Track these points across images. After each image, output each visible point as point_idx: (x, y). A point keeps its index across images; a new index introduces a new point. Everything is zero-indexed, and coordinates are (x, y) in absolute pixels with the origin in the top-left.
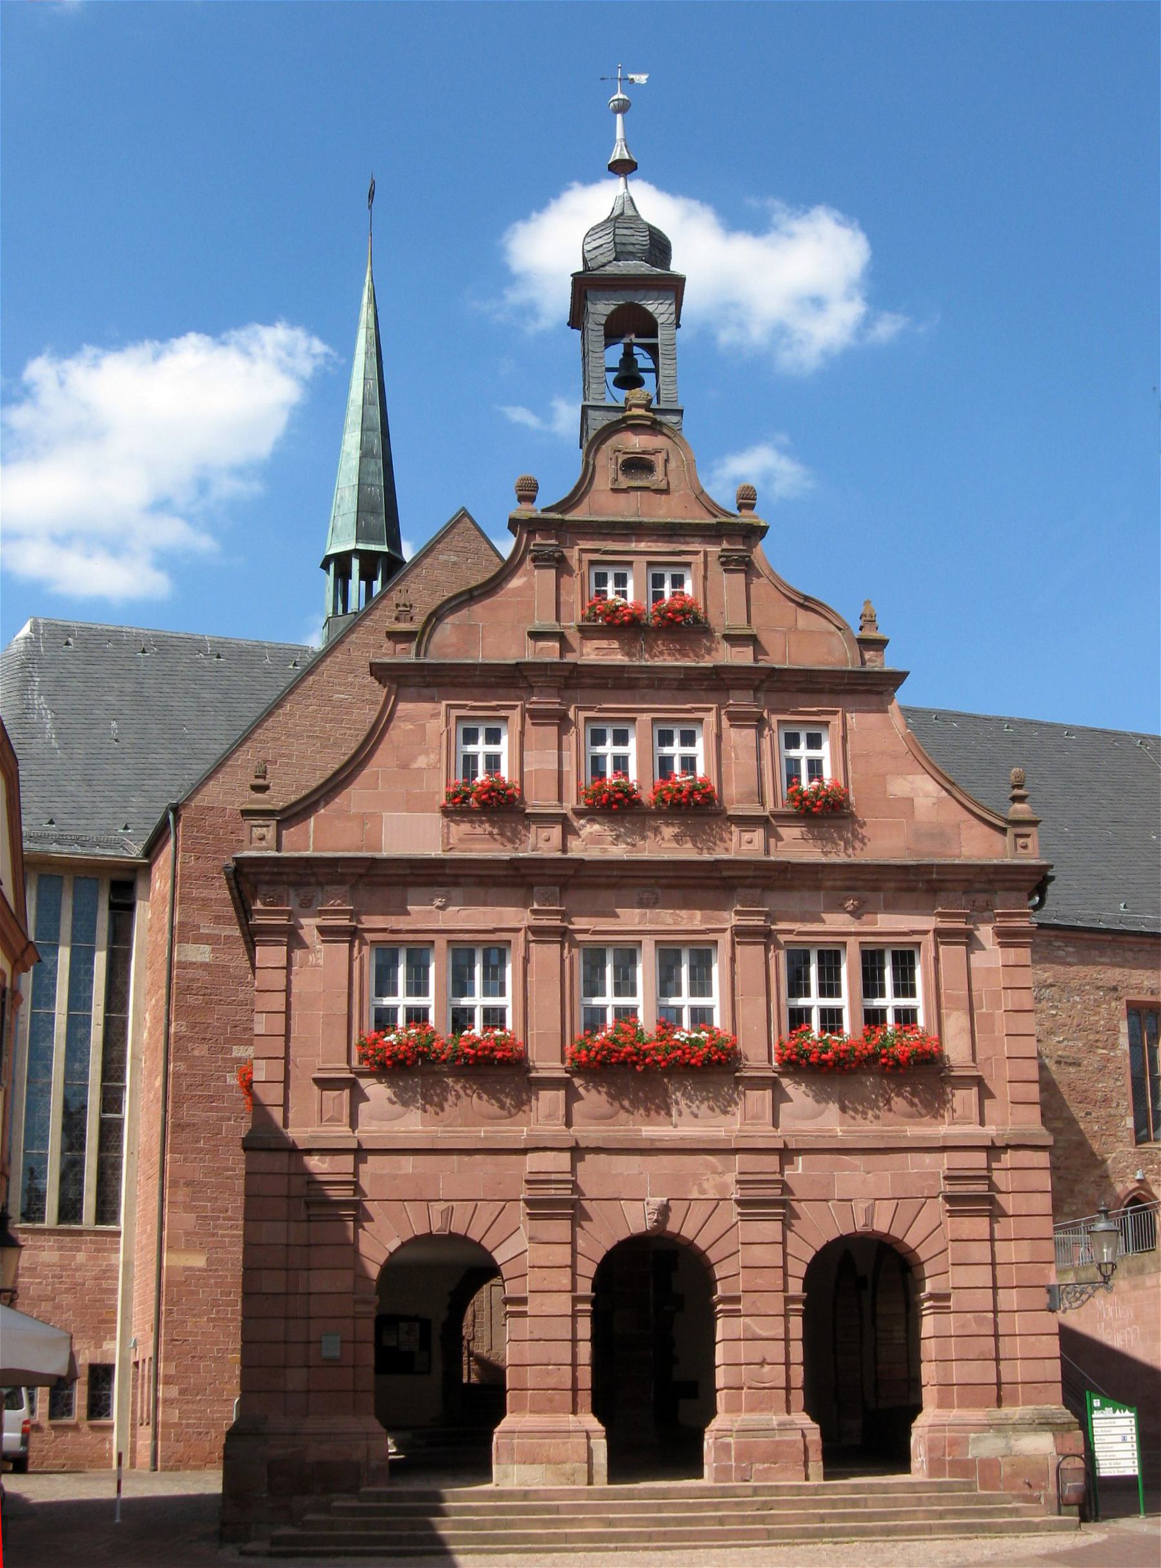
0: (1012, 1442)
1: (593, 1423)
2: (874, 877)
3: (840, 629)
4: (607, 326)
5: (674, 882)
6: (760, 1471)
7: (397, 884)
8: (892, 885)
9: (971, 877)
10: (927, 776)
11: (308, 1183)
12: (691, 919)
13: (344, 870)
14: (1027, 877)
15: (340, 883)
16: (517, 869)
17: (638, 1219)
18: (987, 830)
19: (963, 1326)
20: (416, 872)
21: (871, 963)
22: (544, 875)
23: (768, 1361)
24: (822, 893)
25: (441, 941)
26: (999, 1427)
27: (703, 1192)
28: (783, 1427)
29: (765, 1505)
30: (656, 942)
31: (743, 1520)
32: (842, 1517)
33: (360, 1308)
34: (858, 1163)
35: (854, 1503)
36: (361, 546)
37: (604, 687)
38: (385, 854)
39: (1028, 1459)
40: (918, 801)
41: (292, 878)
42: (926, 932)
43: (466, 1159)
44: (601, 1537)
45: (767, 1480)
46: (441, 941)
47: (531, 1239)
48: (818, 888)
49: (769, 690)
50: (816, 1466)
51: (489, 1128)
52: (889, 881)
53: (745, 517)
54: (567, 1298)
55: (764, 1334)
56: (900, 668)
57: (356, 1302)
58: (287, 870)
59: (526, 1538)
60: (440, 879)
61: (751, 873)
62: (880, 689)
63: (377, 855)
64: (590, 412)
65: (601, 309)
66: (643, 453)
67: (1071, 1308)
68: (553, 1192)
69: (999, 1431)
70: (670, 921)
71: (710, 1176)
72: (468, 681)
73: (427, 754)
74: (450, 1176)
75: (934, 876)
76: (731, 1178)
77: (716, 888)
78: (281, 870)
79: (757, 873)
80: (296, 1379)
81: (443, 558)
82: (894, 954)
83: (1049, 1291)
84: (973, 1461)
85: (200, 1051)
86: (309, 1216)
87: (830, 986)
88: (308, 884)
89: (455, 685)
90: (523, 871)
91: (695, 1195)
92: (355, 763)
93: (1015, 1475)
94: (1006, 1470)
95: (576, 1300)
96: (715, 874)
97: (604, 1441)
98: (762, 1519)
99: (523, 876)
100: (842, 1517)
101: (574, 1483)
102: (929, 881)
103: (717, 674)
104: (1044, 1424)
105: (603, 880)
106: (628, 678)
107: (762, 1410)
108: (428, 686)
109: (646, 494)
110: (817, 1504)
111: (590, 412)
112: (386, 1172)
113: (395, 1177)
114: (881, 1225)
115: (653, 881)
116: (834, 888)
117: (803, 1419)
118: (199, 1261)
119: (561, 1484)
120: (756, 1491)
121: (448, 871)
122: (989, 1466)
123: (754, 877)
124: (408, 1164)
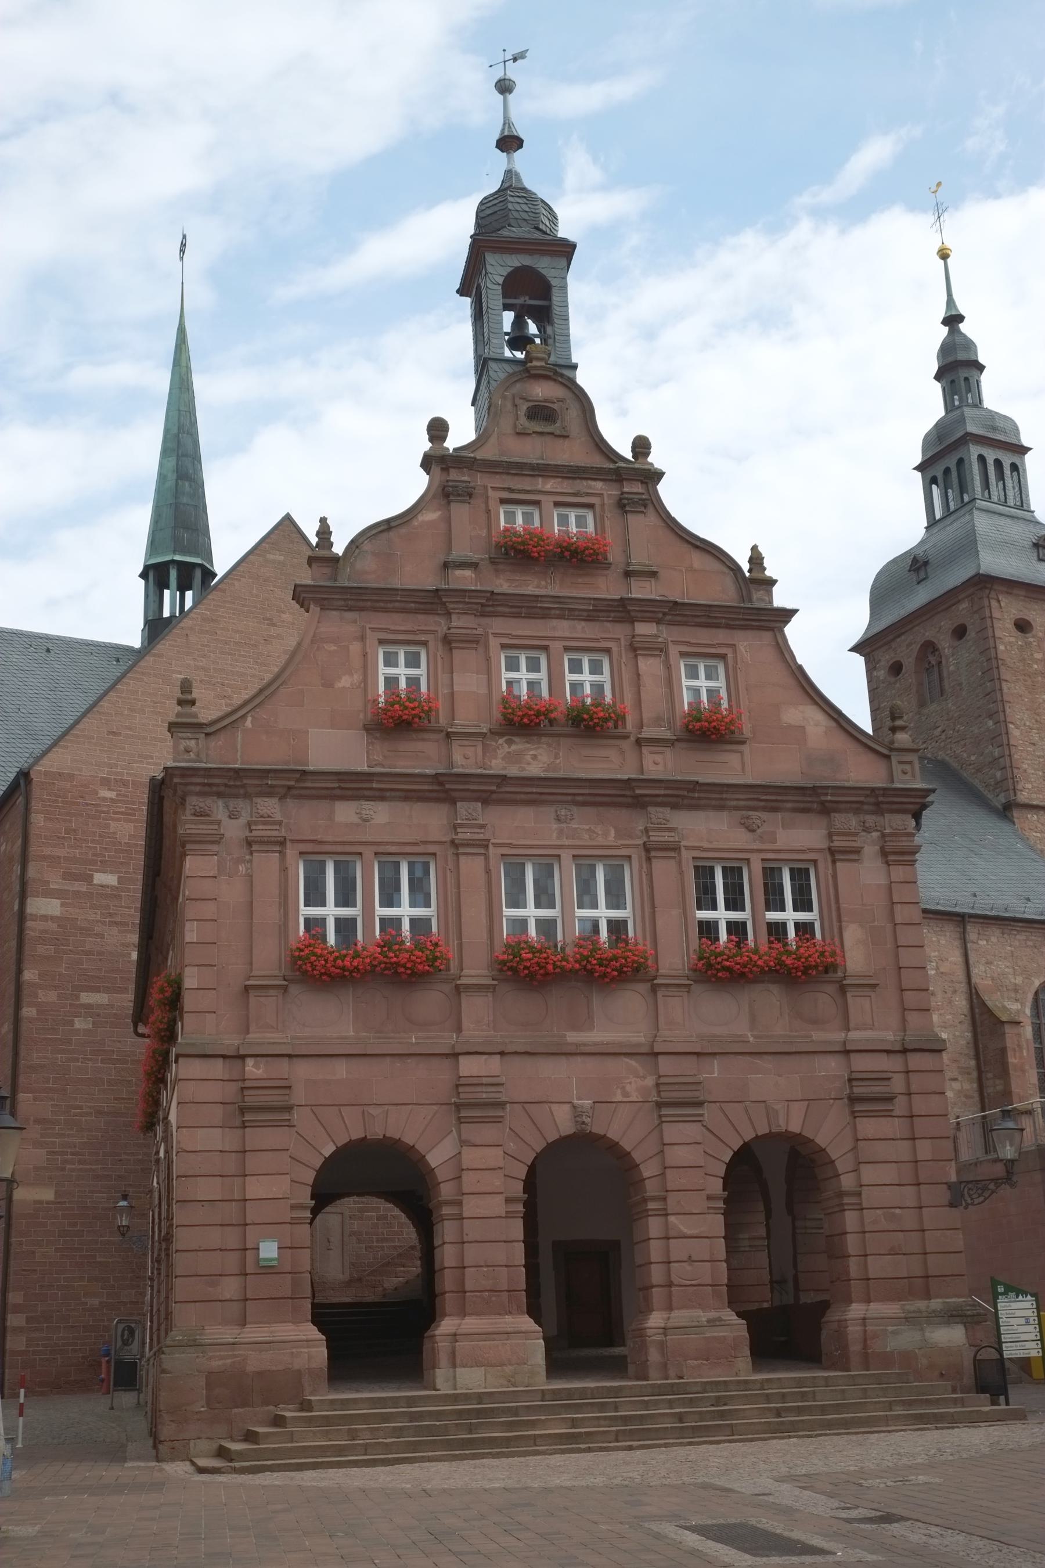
0: (927, 1334)
1: (527, 1323)
3: (732, 570)
4: (504, 286)
8: (789, 805)
9: (862, 799)
10: (815, 707)
11: (242, 1089)
13: (274, 783)
14: (912, 800)
15: (270, 795)
16: (441, 784)
17: (563, 1123)
18: (871, 756)
20: (343, 785)
21: (771, 874)
22: (468, 790)
23: (694, 1258)
24: (725, 813)
26: (911, 1320)
27: (626, 1094)
28: (712, 1323)
29: (718, 1401)
32: (800, 1411)
35: (803, 1396)
36: (177, 558)
37: (517, 616)
38: (311, 768)
40: (811, 730)
41: (222, 789)
42: (821, 850)
44: (507, 1442)
46: (368, 852)
47: (463, 1143)
48: (721, 808)
49: (671, 623)
50: (743, 1362)
51: (419, 1034)
54: (500, 1199)
56: (795, 607)
57: (293, 1207)
58: (217, 781)
60: (367, 793)
61: (662, 792)
62: (773, 624)
66: (546, 401)
67: (972, 1204)
68: (484, 1096)
70: (587, 836)
72: (390, 605)
73: (351, 674)
75: (829, 798)
76: (650, 1081)
77: (627, 806)
78: (211, 781)
81: (270, 557)
82: (792, 871)
85: (52, 996)
87: (735, 900)
88: (236, 796)
89: (375, 610)
90: (447, 786)
91: (619, 1098)
92: (266, 693)
95: (508, 1200)
96: (628, 793)
97: (542, 1341)
99: (447, 791)
100: (800, 1411)
102: (823, 803)
103: (624, 606)
104: (952, 1316)
108: (350, 609)
109: (548, 438)
115: (569, 798)
116: (737, 808)
118: (47, 1194)
119: (502, 1386)
121: (374, 785)
122: (907, 1358)
124: (341, 1070)
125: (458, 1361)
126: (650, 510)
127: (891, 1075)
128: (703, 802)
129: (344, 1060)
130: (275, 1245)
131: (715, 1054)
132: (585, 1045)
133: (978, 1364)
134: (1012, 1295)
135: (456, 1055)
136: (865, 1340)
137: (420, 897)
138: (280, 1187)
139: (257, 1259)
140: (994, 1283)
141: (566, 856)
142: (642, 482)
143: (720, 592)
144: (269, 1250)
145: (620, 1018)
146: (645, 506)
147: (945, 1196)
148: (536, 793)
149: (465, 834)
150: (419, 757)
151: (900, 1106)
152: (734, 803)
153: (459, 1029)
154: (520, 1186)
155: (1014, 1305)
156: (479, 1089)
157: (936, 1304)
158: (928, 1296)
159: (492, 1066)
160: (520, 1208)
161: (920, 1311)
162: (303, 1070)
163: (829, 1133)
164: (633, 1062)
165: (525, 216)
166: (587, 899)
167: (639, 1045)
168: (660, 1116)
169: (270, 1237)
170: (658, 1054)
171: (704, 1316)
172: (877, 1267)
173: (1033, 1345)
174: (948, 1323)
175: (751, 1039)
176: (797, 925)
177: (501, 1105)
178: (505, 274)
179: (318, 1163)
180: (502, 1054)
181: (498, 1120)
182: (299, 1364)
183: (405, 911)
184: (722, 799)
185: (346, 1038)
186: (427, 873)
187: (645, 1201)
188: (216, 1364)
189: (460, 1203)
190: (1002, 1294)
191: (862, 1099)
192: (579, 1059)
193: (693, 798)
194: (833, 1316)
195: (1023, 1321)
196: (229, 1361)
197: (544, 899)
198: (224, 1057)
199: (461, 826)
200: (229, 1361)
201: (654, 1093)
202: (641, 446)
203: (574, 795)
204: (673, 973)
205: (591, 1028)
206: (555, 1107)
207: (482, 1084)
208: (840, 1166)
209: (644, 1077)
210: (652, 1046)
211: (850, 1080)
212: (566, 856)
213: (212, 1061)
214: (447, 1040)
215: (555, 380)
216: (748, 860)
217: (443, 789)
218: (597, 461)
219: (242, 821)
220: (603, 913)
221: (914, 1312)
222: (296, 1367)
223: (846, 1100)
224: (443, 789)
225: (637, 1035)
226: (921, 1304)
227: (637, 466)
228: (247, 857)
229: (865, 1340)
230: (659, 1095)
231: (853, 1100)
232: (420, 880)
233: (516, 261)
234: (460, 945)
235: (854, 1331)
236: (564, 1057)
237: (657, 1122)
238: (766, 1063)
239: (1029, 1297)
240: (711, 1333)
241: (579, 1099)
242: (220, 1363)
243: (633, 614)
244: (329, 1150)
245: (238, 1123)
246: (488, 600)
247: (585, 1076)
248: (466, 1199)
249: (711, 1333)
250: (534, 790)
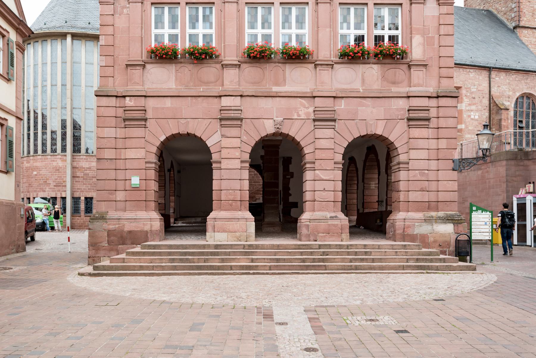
1: (249, 215)
6: (322, 237)
17: (269, 128)
19: (414, 176)
26: (428, 220)
27: (299, 115)
31: (314, 260)
33: (148, 165)
34: (370, 104)
39: (443, 235)
45: (325, 241)
47: (223, 136)
50: (346, 235)
55: (325, 178)
57: (146, 163)
68: (232, 115)
71: (302, 108)
74: (187, 108)
76: (311, 110)
80: (120, 196)
83: (453, 161)
84: (417, 235)
86: (125, 125)
91: (296, 117)
93: (435, 241)
94: (431, 239)
95: (242, 162)
97: (254, 223)
98: (323, 260)
101: (240, 241)
107: (323, 211)
110: (348, 254)
112: (159, 106)
113: (163, 108)
114: (379, 132)
117: (342, 216)
119: (235, 241)
120: (320, 246)
124: (168, 102)
125: (216, 230)
127: (429, 108)
129: (169, 99)
130: (138, 178)
131: (343, 97)
132: (280, 92)
133: (457, 241)
134: (480, 211)
135: (220, 96)
136: (404, 228)
137: (208, 24)
138: (141, 153)
139: (131, 184)
140: (471, 206)
141: (277, 4)
144: (135, 181)
145: (298, 79)
147: (451, 165)
151: (433, 123)
153: (223, 85)
154: (248, 156)
155: (480, 216)
156: (230, 112)
157: (441, 214)
158: (437, 210)
159: (235, 102)
161: (432, 217)
162: (151, 103)
163: (397, 134)
164: (303, 101)
166: (287, 25)
167: (306, 93)
168: (314, 126)
169: (136, 175)
170: (315, 97)
171: (329, 215)
172: (413, 196)
173: (488, 234)
174: (445, 223)
175: (361, 91)
176: (390, 37)
177: (241, 120)
179: (158, 144)
180: (241, 96)
181: (240, 126)
182: (147, 228)
183: (201, 30)
186: (211, 12)
187: (305, 164)
188: (111, 227)
189: (220, 162)
190: (474, 211)
191: (416, 119)
192: (278, 99)
194: (392, 217)
195: (484, 223)
196: (117, 226)
197: (266, 25)
198: (117, 97)
200: (117, 226)
201: (312, 115)
204: (326, 59)
205: (285, 85)
206: (265, 121)
208: (400, 150)
209: (308, 108)
210: (312, 93)
211: (409, 110)
212: (277, 4)
213: (111, 98)
214: (216, 90)
220: (294, 31)
221: (429, 217)
222: (145, 229)
223: (406, 120)
225: (306, 88)
226: (434, 214)
228: (128, 6)
229: (404, 228)
230: (314, 116)
231: (409, 120)
232: (208, 16)
234: (224, 46)
235: (399, 224)
236: (270, 98)
237: (313, 128)
238: (369, 102)
239: (488, 213)
240: (330, 222)
241: (277, 117)
242: (113, 226)
244: (163, 138)
245: (123, 126)
247: (281, 106)
248: (222, 161)
249: (330, 222)
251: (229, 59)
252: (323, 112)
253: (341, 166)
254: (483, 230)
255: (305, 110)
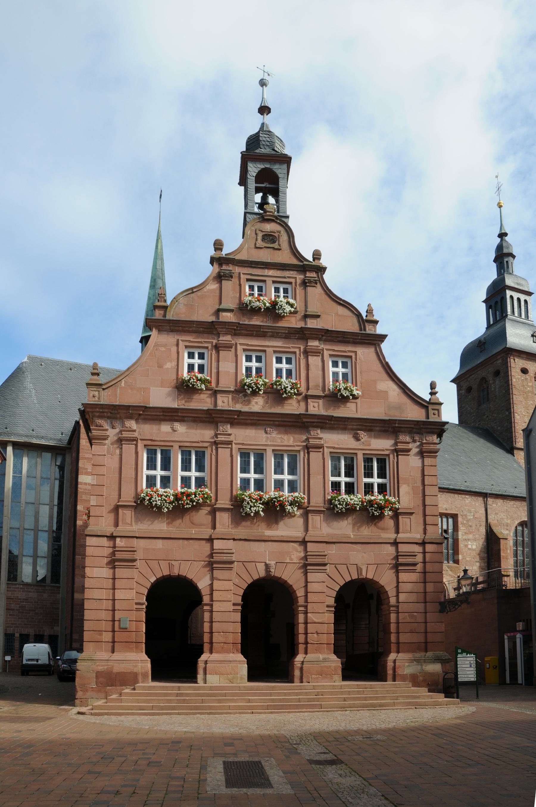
0: (424, 667)
2: (370, 424)
5: (282, 423)
7: (156, 420)
12: (289, 440)
21: (368, 460)
25: (176, 446)
27: (291, 559)
28: (325, 660)
30: (273, 450)
43: (186, 542)
50: (338, 677)
51: (197, 530)
52: (377, 426)
53: (315, 263)
55: (317, 621)
59: (210, 708)
61: (316, 420)
63: (148, 406)
64: (248, 215)
65: (253, 169)
69: (418, 662)
70: (279, 441)
71: (295, 553)
76: (302, 554)
77: (300, 427)
79: (320, 421)
90: (213, 415)
91: (288, 561)
96: (299, 421)
103: (303, 332)
105: (250, 421)
106: (263, 331)
111: (248, 215)
115: (272, 422)
116: (352, 429)
123: (317, 422)
124: (160, 544)
126: (318, 285)
128: (335, 426)
129: (161, 541)
132: (273, 537)
142: (316, 272)
143: (350, 325)
146: (316, 283)
148: (256, 420)
149: (221, 438)
150: (202, 402)
152: (351, 427)
153: (214, 527)
160: (239, 608)
164: (296, 545)
165: (268, 144)
175: (352, 536)
177: (232, 562)
178: (257, 171)
179: (149, 585)
181: (231, 569)
184: (345, 425)
185: (163, 530)
192: (270, 543)
193: (331, 424)
199: (220, 434)
202: (317, 255)
203: (274, 421)
204: (317, 505)
207: (224, 553)
210: (304, 538)
215: (276, 222)
216: (356, 454)
217: (212, 418)
218: (295, 261)
219: (117, 430)
224: (212, 418)
225: (299, 534)
227: (314, 263)
233: (261, 166)
241: (269, 560)
243: (307, 335)
244: (153, 579)
246: (237, 327)
250: (255, 418)
251: (222, 502)
252: (315, 557)
253: (333, 609)
254: (468, 673)
255: (296, 554)
